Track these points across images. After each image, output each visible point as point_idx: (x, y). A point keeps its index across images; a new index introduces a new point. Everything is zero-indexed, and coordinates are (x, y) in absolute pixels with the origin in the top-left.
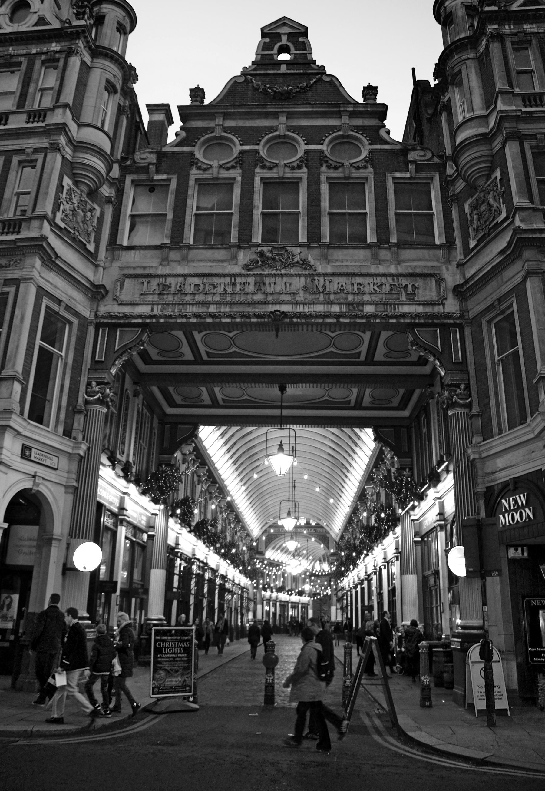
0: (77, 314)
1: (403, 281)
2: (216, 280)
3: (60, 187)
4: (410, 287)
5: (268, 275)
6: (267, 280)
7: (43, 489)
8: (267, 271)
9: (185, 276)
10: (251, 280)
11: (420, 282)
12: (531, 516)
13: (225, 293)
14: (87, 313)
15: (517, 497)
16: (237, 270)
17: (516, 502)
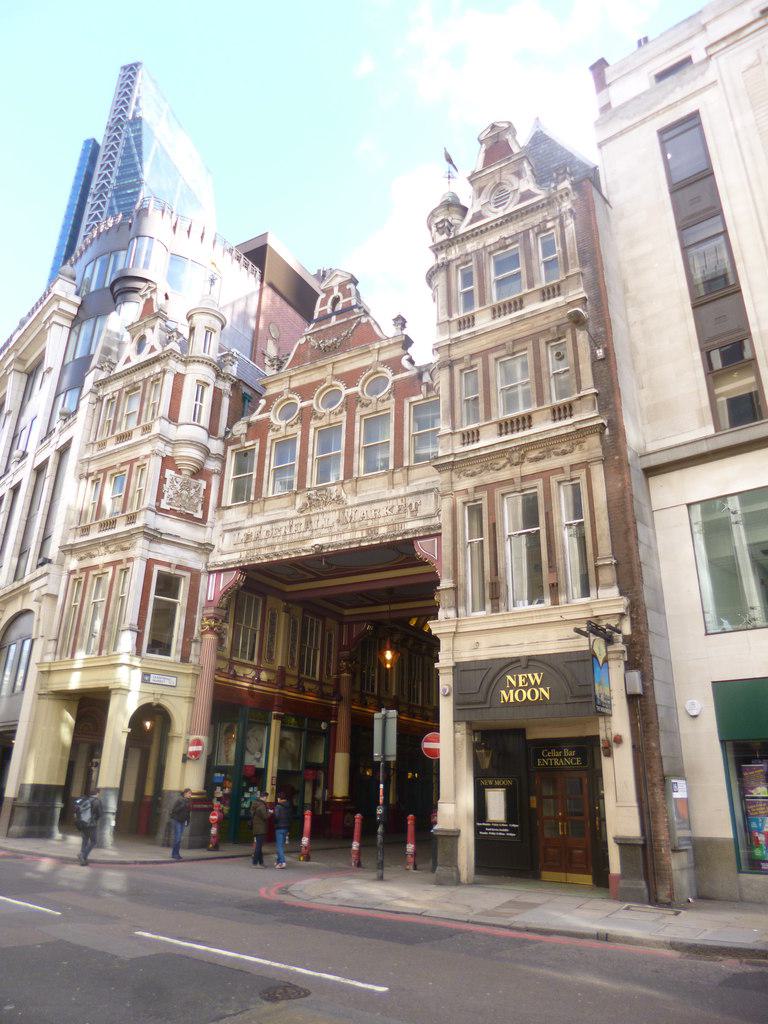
0: (188, 569)
1: (410, 500)
2: (280, 524)
3: (162, 480)
4: (414, 505)
5: (313, 515)
6: (313, 519)
7: (164, 702)
8: (314, 511)
9: (261, 525)
10: (303, 521)
11: (422, 497)
12: (547, 695)
13: (285, 534)
14: (200, 566)
15: (530, 675)
16: (294, 513)
17: (527, 679)
